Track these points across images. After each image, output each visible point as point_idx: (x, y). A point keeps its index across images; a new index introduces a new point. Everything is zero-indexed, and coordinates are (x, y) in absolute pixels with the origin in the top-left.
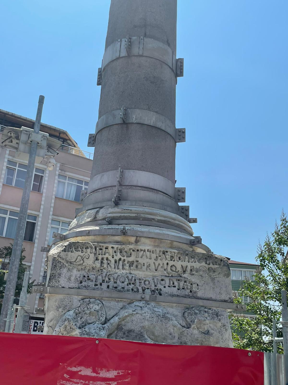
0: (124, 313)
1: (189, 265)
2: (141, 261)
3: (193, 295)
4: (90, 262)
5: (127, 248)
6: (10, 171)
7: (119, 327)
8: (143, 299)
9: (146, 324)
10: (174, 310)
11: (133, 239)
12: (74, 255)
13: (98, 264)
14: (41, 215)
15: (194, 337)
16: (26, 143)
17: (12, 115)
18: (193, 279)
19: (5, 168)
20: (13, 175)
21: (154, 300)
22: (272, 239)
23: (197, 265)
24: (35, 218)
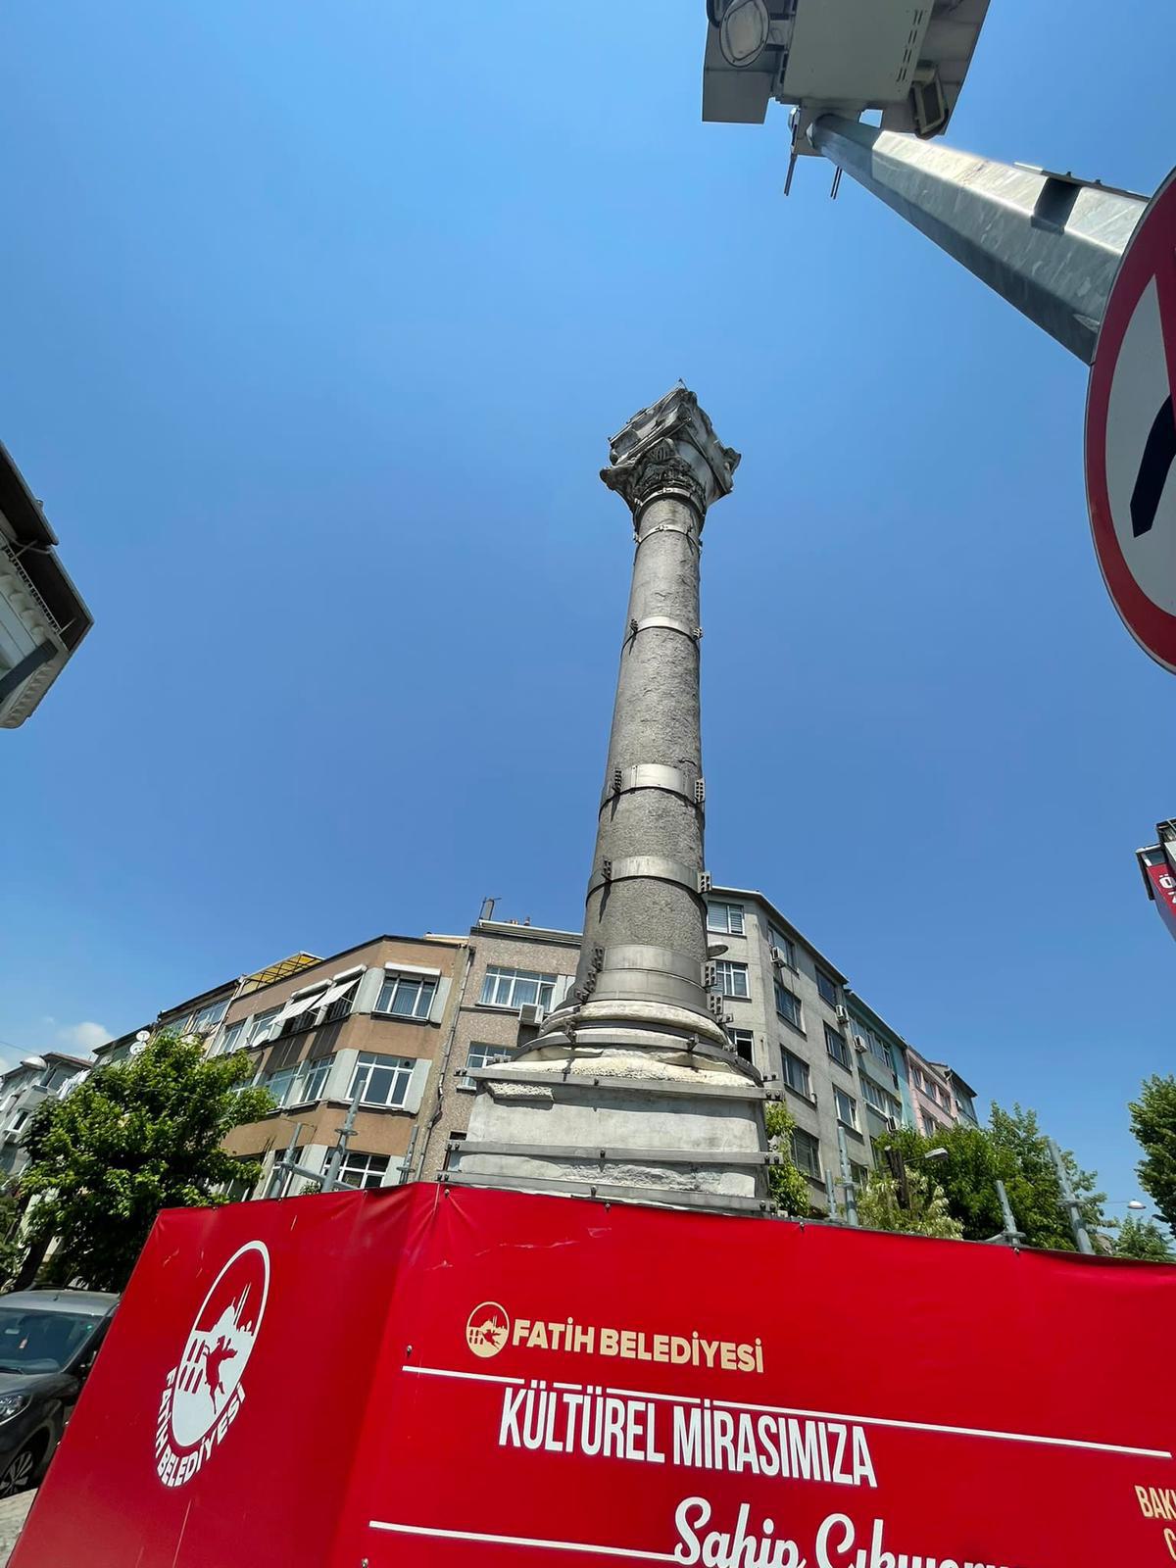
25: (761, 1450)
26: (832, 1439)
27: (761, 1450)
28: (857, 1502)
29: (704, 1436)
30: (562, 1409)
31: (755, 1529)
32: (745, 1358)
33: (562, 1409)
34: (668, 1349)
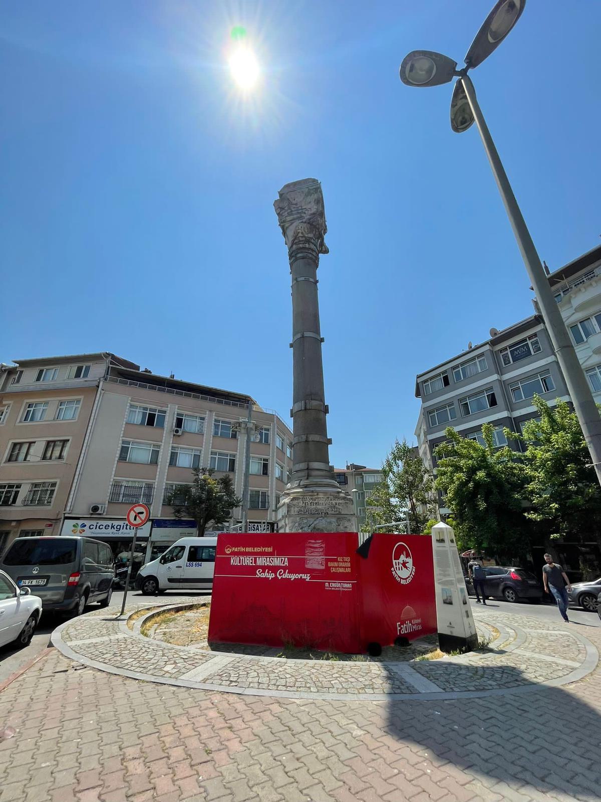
0: (315, 523)
1: (338, 502)
2: (320, 502)
3: (340, 514)
4: (301, 504)
5: (314, 497)
6: (216, 426)
7: (314, 528)
8: (322, 517)
9: (324, 526)
10: (334, 520)
11: (316, 494)
12: (295, 502)
13: (304, 505)
14: (238, 454)
15: (341, 529)
16: (245, 428)
17: (216, 390)
18: (340, 507)
19: (213, 425)
20: (218, 429)
21: (326, 516)
22: (391, 457)
23: (341, 501)
24: (234, 456)
25: (270, 562)
26: (282, 560)
27: (270, 562)
28: (285, 568)
29: (261, 561)
30: (240, 559)
31: (268, 572)
32: (270, 550)
33: (240, 559)
34: (257, 550)
